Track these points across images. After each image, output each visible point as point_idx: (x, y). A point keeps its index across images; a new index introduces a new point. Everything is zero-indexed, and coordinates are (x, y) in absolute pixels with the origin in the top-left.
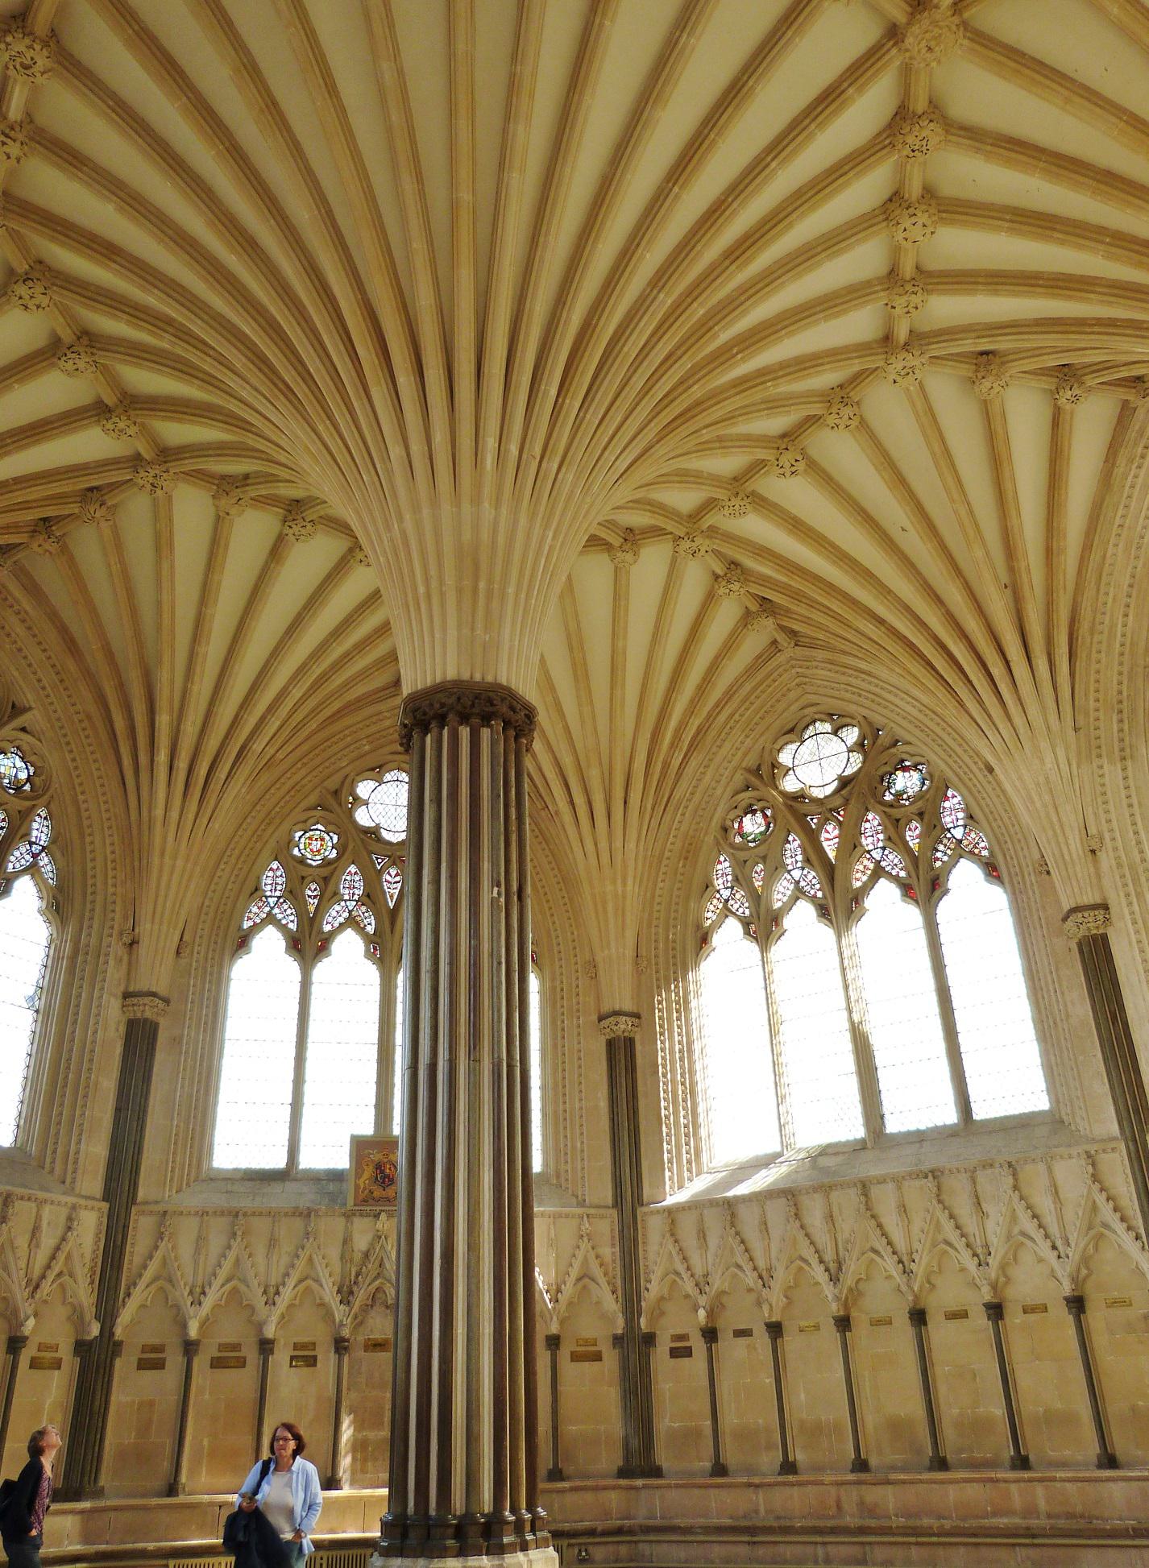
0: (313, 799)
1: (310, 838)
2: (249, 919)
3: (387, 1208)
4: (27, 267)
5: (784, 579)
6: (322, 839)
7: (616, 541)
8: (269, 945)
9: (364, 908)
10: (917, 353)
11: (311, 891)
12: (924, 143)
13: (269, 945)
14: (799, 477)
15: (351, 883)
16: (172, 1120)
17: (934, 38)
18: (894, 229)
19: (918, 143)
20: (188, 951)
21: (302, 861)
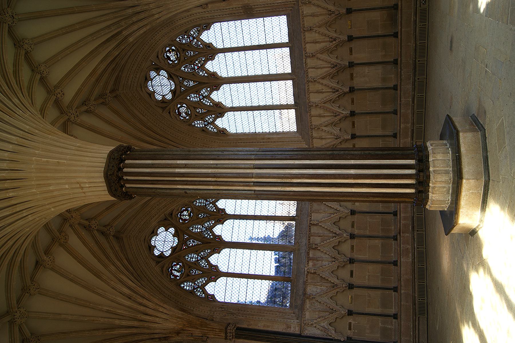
8: (220, 123)
13: (220, 123)
15: (193, 98)
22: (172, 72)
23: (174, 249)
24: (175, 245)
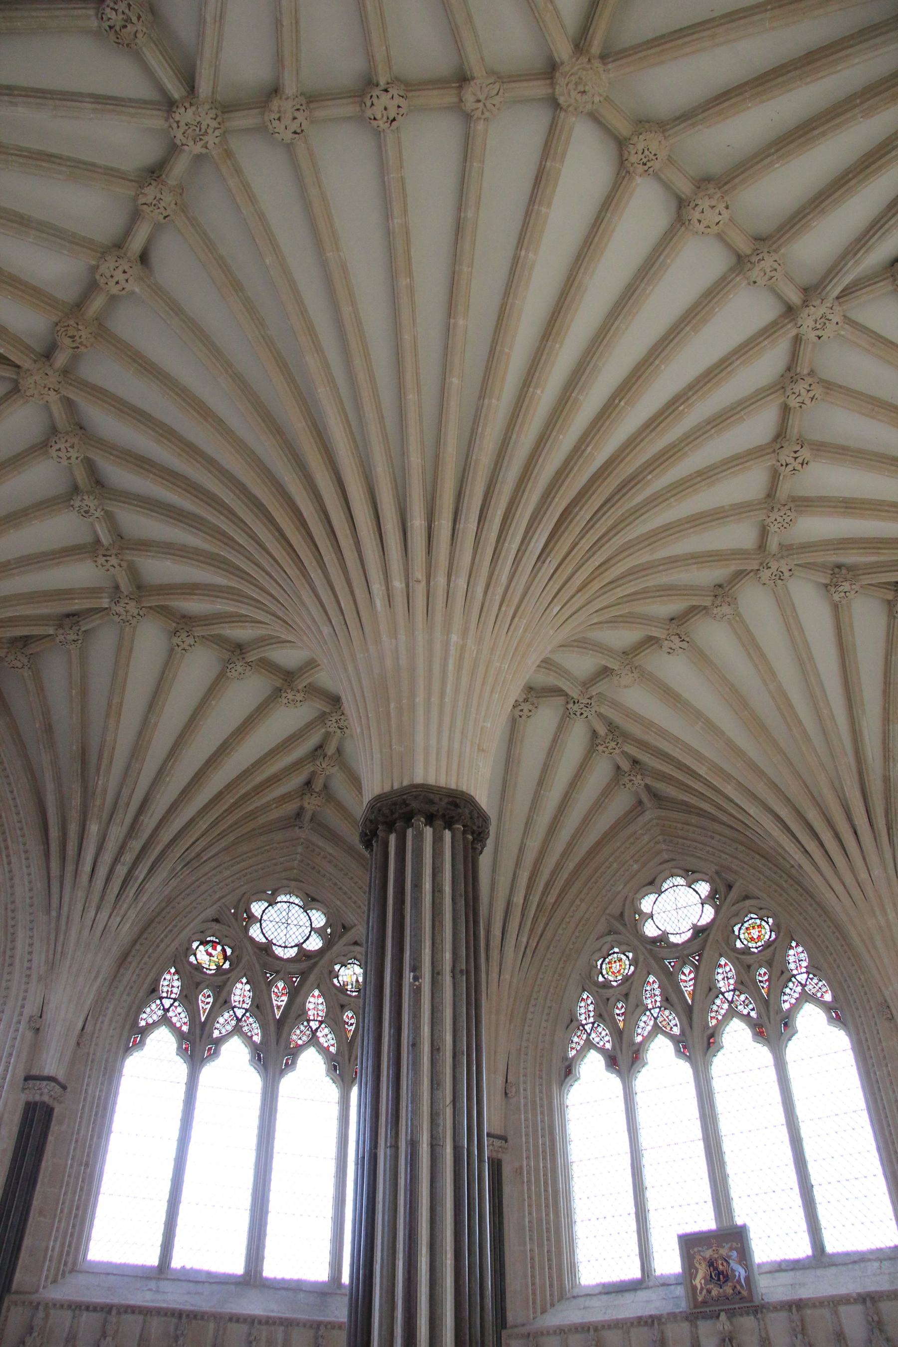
0: (602, 927)
1: (609, 963)
2: (572, 1048)
3: (726, 1307)
4: (174, 625)
5: (873, 559)
6: (620, 960)
7: (707, 601)
9: (667, 1012)
10: (818, 302)
11: (619, 1009)
12: (646, 152)
14: (811, 464)
16: (525, 1245)
17: (576, 84)
18: (691, 227)
19: (643, 157)
20: (514, 1090)
21: (606, 985)
22: (711, 937)
23: (266, 949)
24: (279, 952)
